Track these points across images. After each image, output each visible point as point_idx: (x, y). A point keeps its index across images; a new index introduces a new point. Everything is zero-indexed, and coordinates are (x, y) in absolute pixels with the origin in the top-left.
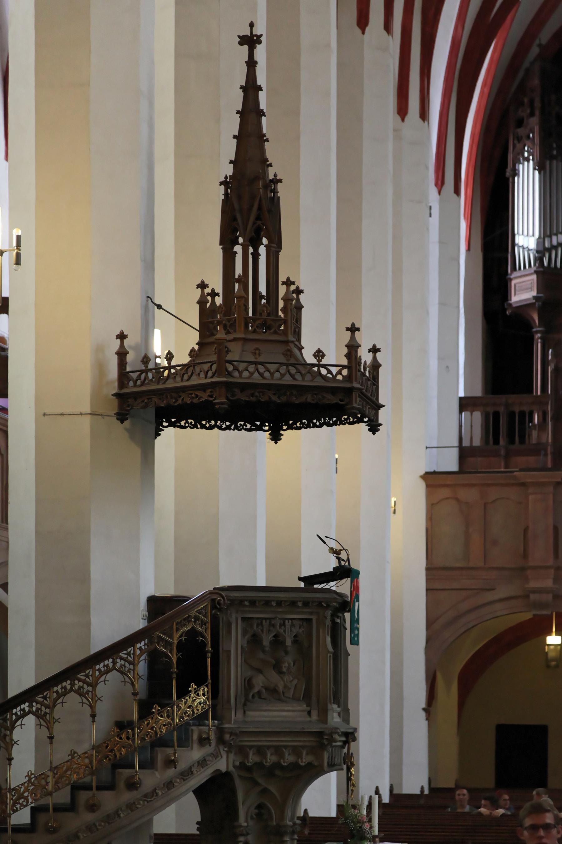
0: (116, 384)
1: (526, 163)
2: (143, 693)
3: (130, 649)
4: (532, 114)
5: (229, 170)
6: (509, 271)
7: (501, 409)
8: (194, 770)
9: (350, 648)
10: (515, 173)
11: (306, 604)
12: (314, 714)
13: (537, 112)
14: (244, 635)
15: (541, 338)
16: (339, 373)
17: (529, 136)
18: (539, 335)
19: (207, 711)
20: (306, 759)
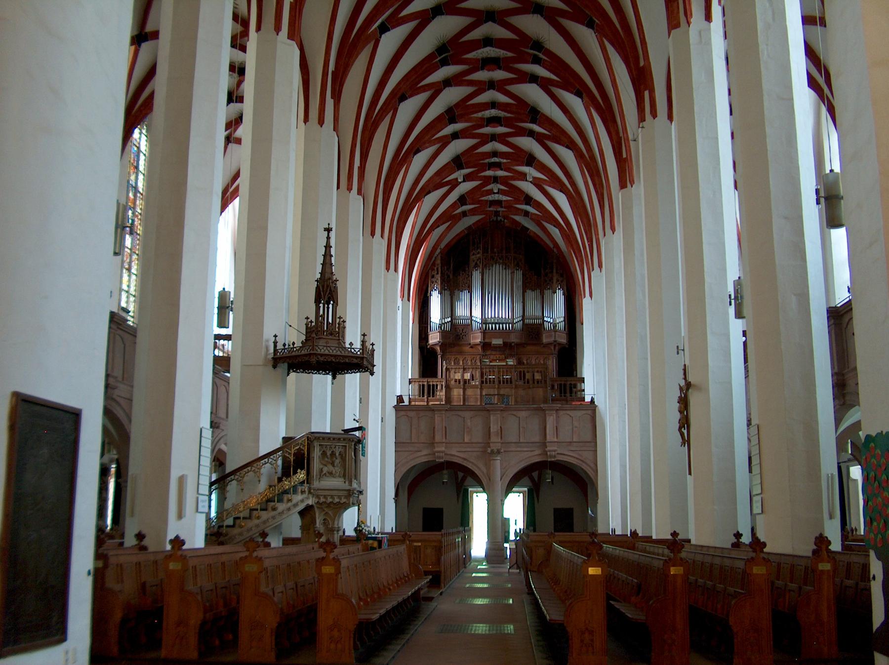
0: (273, 354)
2: (279, 474)
3: (275, 455)
5: (319, 276)
7: (425, 383)
8: (299, 504)
9: (361, 457)
11: (344, 439)
12: (347, 483)
13: (439, 273)
14: (320, 451)
16: (359, 351)
19: (304, 480)
20: (343, 500)
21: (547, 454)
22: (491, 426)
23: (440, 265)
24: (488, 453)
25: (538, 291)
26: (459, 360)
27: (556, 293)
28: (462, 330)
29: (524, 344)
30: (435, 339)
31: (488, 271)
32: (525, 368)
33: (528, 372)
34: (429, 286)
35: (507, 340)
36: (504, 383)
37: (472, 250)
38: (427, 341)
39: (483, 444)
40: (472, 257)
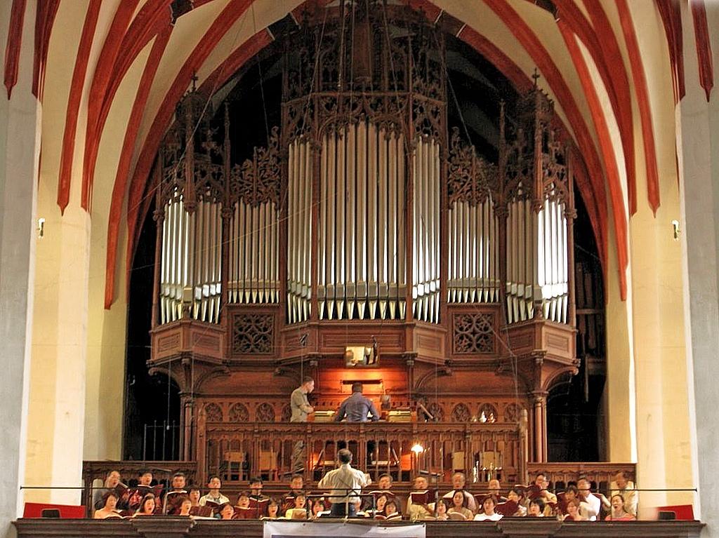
6: (153, 324)
10: (163, 215)
27: (543, 208)
38: (148, 354)
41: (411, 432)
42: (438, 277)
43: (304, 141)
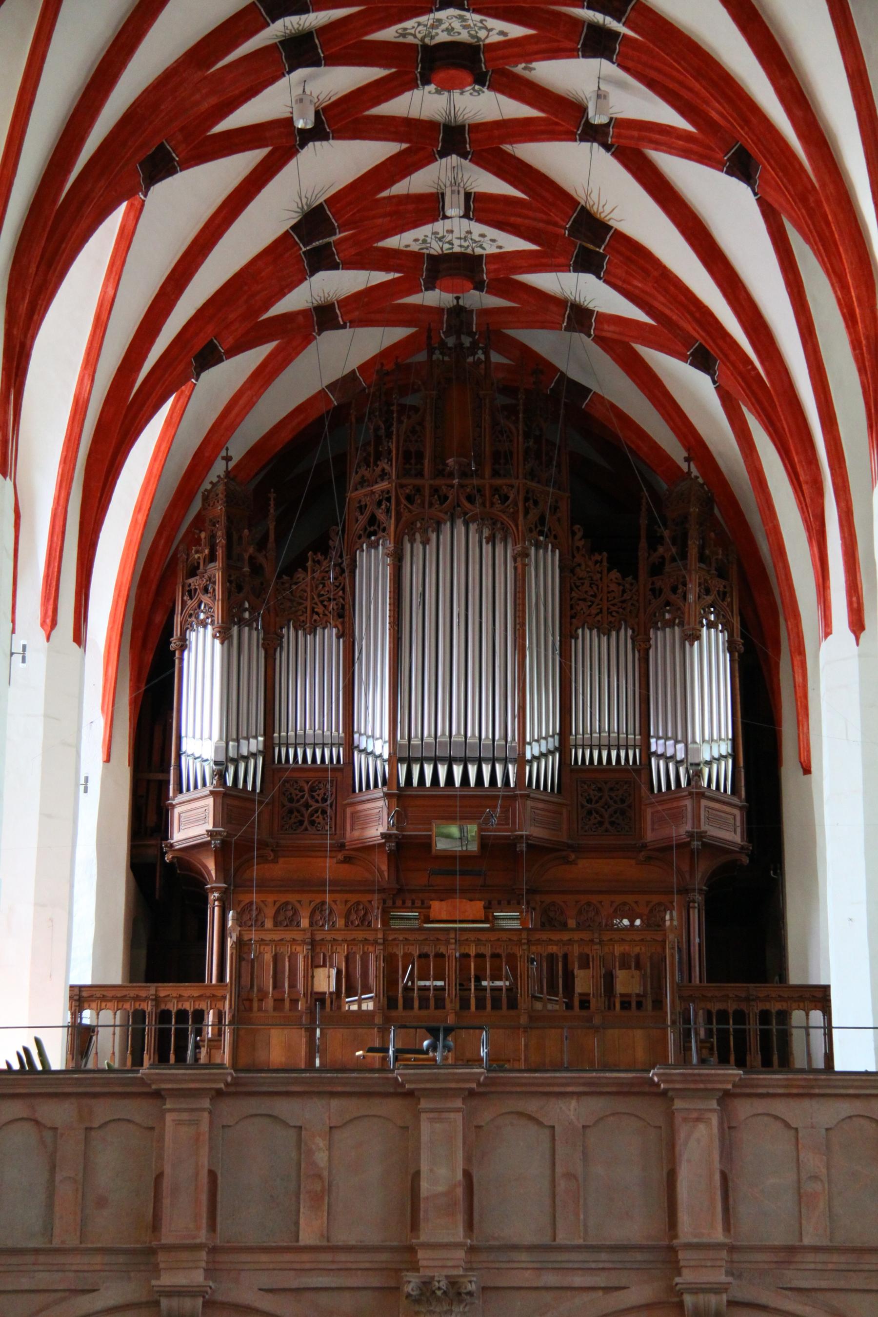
1: (201, 630)
4: (212, 558)
6: (171, 794)
7: (148, 1007)
10: (184, 645)
13: (220, 553)
15: (218, 899)
17: (206, 590)
18: (216, 895)
21: (681, 1305)
22: (424, 1168)
23: (223, 519)
24: (408, 1296)
25: (626, 634)
26: (295, 912)
27: (698, 638)
28: (312, 790)
29: (570, 847)
30: (196, 821)
31: (418, 547)
32: (570, 942)
33: (585, 963)
34: (178, 608)
35: (496, 830)
36: (481, 1005)
37: (359, 466)
39: (384, 1257)
40: (355, 495)
41: (520, 941)
42: (558, 731)
43: (375, 546)
